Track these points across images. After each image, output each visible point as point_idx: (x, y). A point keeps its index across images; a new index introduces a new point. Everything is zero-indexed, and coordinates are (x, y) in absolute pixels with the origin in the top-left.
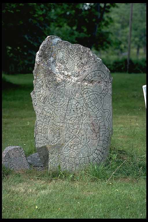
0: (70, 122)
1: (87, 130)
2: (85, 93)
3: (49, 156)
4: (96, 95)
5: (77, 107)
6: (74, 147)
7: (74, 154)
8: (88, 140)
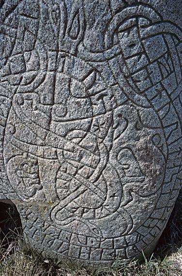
0: (69, 145)
1: (123, 169)
2: (122, 27)
3: (22, 221)
4: (168, 37)
5: (90, 91)
6: (83, 212)
7: (84, 230)
8: (126, 199)
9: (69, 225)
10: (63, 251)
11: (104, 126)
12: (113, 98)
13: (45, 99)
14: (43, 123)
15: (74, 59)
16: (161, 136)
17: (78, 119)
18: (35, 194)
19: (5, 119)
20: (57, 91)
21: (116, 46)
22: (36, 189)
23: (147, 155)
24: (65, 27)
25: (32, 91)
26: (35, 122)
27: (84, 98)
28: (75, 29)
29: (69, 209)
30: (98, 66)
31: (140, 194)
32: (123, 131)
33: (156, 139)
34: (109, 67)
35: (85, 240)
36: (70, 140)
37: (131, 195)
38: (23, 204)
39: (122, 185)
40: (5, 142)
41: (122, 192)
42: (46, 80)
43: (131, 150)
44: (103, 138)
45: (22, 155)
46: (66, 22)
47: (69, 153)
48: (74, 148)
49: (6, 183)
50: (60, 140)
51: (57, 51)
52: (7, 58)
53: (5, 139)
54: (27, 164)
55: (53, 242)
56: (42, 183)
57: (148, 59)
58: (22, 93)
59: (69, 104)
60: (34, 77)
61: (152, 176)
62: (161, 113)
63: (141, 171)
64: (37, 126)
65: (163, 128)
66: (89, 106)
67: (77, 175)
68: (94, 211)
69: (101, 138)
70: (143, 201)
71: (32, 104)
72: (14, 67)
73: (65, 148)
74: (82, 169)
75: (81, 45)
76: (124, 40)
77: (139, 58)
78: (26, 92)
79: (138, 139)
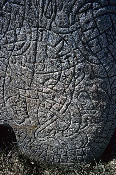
0: (46, 89)
1: (82, 105)
3: (16, 138)
5: (60, 53)
6: (55, 133)
7: (56, 144)
8: (83, 124)
9: (46, 141)
10: (43, 157)
11: (69, 77)
12: (75, 58)
13: (30, 59)
14: (29, 75)
15: (49, 32)
16: (107, 83)
17: (52, 72)
18: (25, 120)
19: (5, 73)
20: (37, 54)
21: (77, 23)
22: (25, 118)
23: (98, 96)
24: (43, 11)
25: (22, 54)
26: (24, 75)
27: (55, 58)
28: (49, 11)
29: (47, 130)
30: (65, 36)
31: (93, 121)
32: (82, 80)
33: (104, 85)
34: (72, 37)
35: (57, 150)
36: (47, 86)
37: (87, 122)
38: (17, 127)
39: (81, 115)
40: (5, 88)
41: (81, 119)
42: (30, 47)
43: (87, 92)
44: (69, 85)
45: (16, 96)
46: (43, 7)
47: (46, 94)
48: (49, 91)
49: (6, 114)
50: (40, 86)
51: (38, 27)
52: (5, 33)
53: (5, 86)
54: (19, 102)
55: (36, 151)
56: (29, 114)
57: (99, 32)
58: (15, 55)
59: (46, 63)
60: (23, 45)
61: (101, 110)
62: (107, 68)
63: (93, 106)
64: (25, 77)
65: (108, 78)
66: (59, 64)
67: (51, 109)
68: (63, 132)
69: (67, 85)
70: (95, 126)
71: (21, 63)
72: (9, 38)
73: (43, 91)
74: (55, 105)
75: (53, 23)
76: (83, 18)
77: (93, 31)
78: (18, 55)
79: (92, 85)
